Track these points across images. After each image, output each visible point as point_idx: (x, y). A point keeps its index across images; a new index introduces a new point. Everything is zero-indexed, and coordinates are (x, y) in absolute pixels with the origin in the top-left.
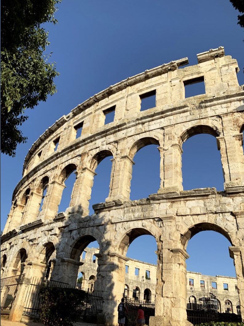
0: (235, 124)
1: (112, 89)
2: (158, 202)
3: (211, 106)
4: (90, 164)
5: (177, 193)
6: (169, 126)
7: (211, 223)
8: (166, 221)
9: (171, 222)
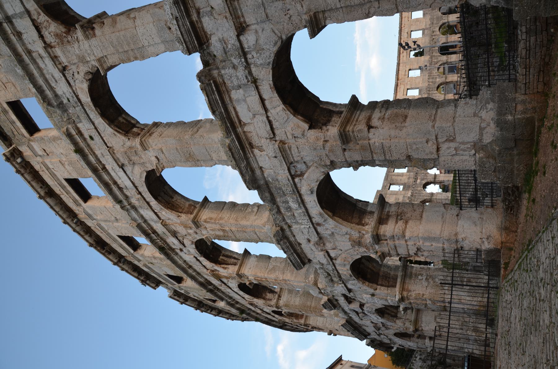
0: (65, 40)
1: (94, 243)
2: (258, 172)
3: (52, 88)
4: (230, 266)
5: (229, 144)
6: (113, 157)
7: (271, 73)
8: (291, 156)
9: (290, 148)
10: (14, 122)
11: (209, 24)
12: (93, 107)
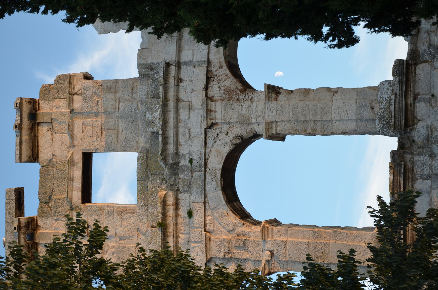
0: (236, 97)
3: (177, 144)
10: (72, 180)
11: (422, 110)
12: (219, 176)
